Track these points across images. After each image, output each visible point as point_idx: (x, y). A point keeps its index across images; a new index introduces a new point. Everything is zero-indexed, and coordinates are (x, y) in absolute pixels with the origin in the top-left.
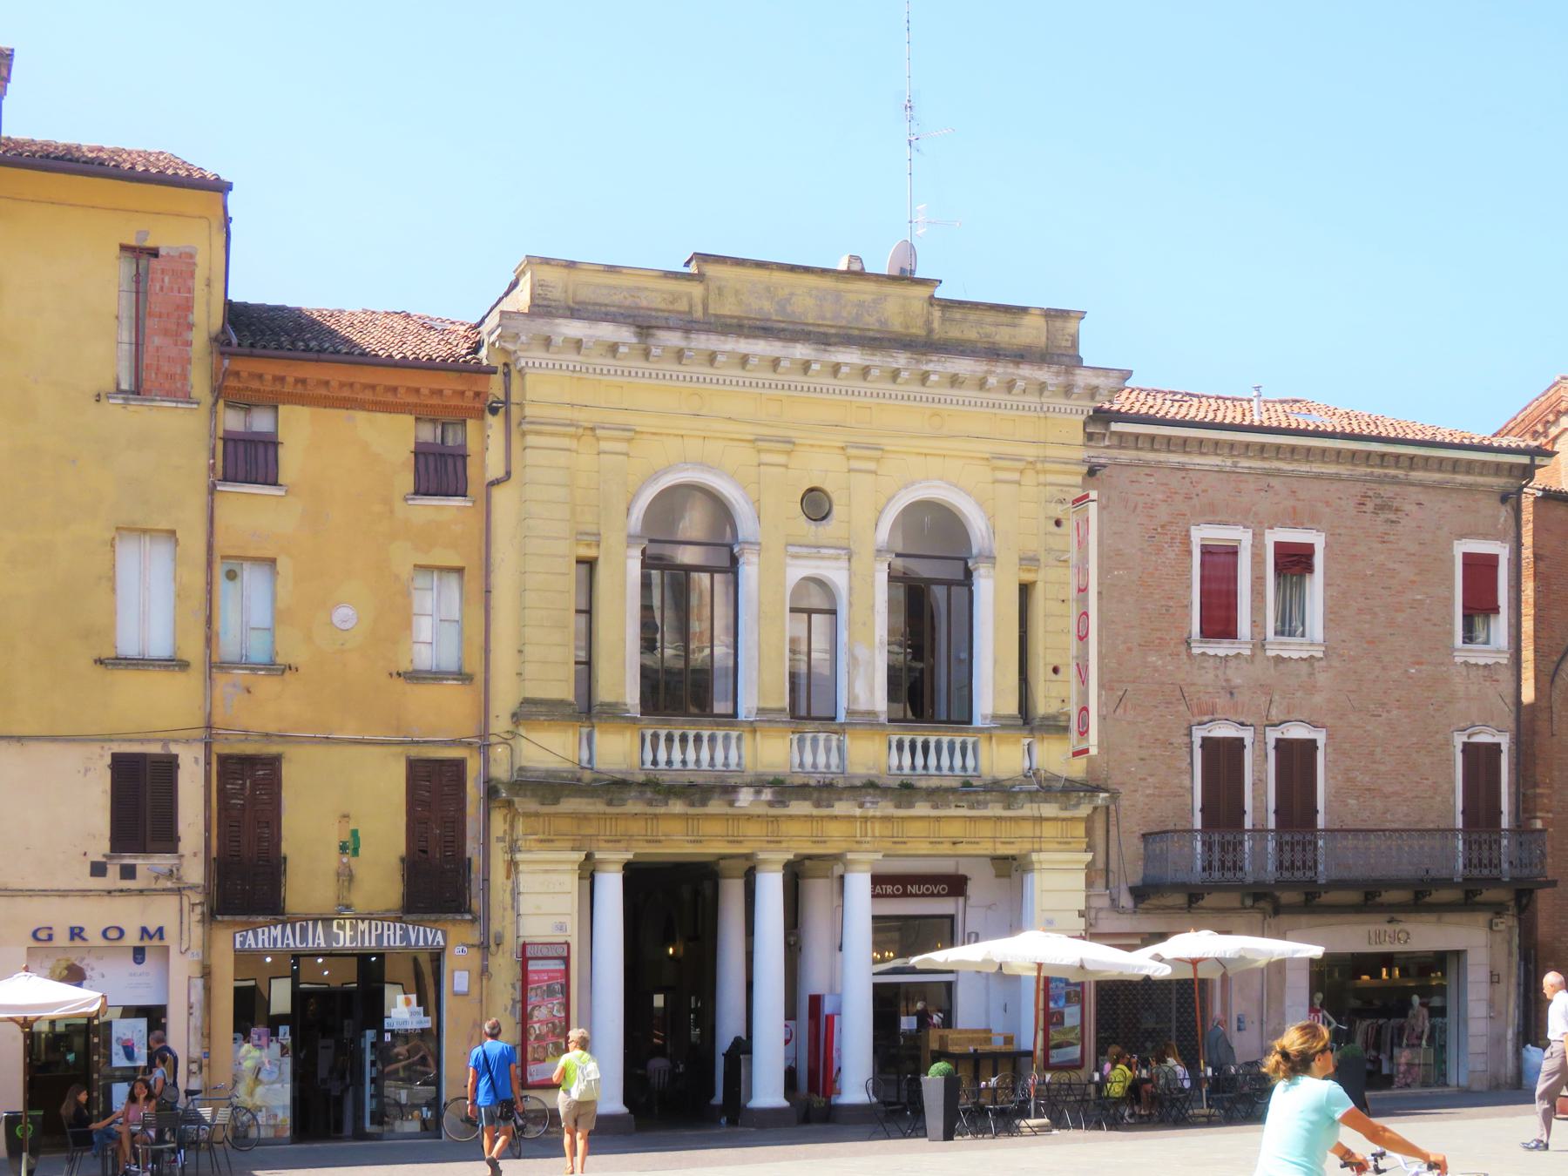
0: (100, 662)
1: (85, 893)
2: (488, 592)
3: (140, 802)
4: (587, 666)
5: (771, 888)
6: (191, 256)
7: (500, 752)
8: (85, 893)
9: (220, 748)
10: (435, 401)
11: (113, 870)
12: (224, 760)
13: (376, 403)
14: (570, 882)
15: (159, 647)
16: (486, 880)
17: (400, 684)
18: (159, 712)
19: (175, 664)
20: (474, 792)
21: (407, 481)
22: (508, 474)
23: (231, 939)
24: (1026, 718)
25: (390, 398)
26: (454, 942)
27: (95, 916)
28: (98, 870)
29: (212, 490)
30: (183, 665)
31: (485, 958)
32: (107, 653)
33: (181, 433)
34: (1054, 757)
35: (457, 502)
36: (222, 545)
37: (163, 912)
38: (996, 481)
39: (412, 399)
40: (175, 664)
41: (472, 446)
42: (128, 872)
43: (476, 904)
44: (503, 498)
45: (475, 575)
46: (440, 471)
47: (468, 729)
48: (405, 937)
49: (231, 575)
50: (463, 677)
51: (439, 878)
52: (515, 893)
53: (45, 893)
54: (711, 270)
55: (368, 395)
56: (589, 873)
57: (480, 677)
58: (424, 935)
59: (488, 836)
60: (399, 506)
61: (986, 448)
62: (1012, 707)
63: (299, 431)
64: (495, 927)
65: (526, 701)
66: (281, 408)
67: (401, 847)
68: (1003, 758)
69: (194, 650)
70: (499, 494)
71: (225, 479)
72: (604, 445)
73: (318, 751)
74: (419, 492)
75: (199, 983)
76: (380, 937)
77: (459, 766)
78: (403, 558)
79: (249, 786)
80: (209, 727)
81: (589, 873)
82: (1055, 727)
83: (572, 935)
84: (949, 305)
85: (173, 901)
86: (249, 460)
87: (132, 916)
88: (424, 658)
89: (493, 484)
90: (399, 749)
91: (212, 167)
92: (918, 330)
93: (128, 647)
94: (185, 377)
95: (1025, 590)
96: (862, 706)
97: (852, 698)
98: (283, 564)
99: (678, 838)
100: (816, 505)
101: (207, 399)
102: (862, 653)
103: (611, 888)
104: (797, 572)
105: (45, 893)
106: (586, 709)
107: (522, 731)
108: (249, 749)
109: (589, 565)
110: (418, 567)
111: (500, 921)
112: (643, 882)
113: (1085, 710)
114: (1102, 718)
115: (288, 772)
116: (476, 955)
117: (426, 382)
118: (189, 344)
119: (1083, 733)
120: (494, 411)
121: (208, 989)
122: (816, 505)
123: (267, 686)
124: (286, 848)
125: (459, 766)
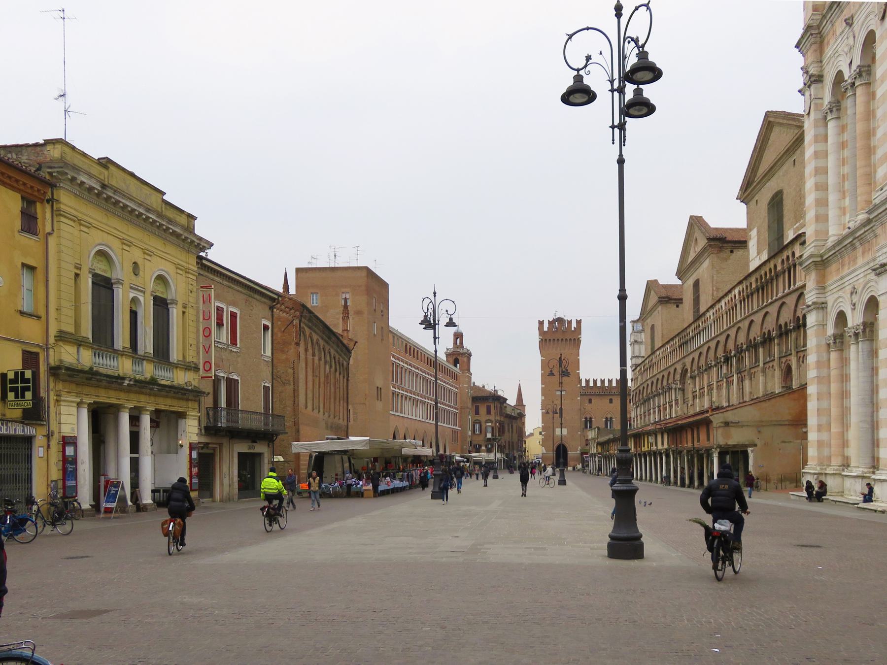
2: (47, 281)
7: (51, 352)
13: (10, 185)
16: (48, 407)
17: (18, 315)
20: (43, 369)
21: (18, 224)
22: (53, 230)
25: (15, 185)
26: (38, 434)
31: (49, 441)
39: (22, 187)
41: (39, 215)
44: (52, 241)
48: (23, 431)
54: (112, 168)
55: (7, 181)
58: (29, 431)
64: (51, 429)
65: (61, 331)
76: (15, 430)
89: (50, 234)
111: (53, 427)
116: (45, 439)
120: (48, 201)
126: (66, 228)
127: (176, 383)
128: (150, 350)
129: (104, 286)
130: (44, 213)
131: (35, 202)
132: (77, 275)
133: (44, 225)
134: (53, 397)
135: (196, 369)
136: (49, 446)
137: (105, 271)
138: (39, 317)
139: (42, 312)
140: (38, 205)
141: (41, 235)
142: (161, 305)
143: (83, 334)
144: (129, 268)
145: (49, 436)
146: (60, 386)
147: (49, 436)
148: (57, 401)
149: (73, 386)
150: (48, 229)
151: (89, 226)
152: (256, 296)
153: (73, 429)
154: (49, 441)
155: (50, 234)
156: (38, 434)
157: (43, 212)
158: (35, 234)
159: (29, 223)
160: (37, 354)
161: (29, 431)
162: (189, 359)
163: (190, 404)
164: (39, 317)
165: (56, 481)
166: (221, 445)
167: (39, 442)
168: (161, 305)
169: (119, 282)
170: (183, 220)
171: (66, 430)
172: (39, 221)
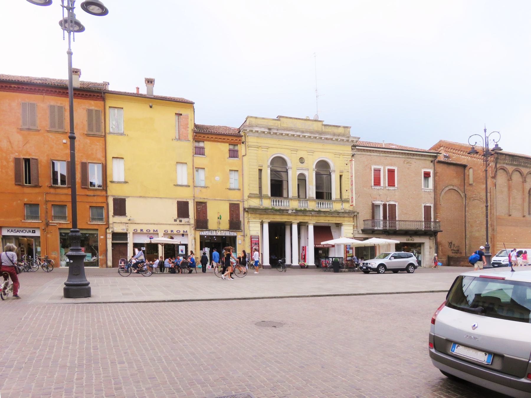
1: (173, 224)
3: (182, 209)
4: (260, 188)
5: (295, 228)
7: (246, 203)
8: (173, 224)
9: (197, 200)
10: (232, 141)
11: (178, 221)
12: (197, 202)
14: (259, 225)
15: (185, 183)
17: (228, 190)
18: (185, 195)
19: (188, 186)
20: (241, 210)
21: (228, 155)
23: (199, 233)
24: (341, 200)
27: (175, 229)
28: (175, 220)
30: (189, 186)
32: (175, 184)
33: (188, 146)
34: (347, 207)
36: (195, 166)
37: (187, 228)
40: (188, 186)
41: (239, 150)
42: (181, 221)
43: (242, 228)
46: (233, 154)
49: (197, 171)
50: (239, 190)
51: (235, 224)
52: (249, 227)
53: (166, 224)
56: (262, 224)
57: (242, 189)
59: (244, 217)
62: (339, 197)
63: (208, 146)
64: (246, 233)
67: (229, 219)
68: (337, 207)
69: (191, 184)
70: (244, 158)
75: (194, 240)
77: (238, 205)
78: (227, 169)
79: (202, 206)
81: (262, 224)
82: (347, 201)
83: (259, 234)
84: (325, 125)
85: (189, 226)
86: (199, 151)
87: (182, 229)
88: (232, 186)
91: (190, 99)
92: (320, 130)
93: (180, 183)
95: (341, 176)
96: (311, 196)
97: (309, 195)
99: (278, 219)
100: (302, 160)
102: (311, 187)
103: (266, 227)
104: (299, 172)
105: (166, 224)
106: (260, 196)
108: (201, 201)
109: (260, 170)
110: (230, 170)
112: (272, 226)
113: (352, 198)
114: (356, 199)
115: (208, 205)
116: (242, 237)
117: (230, 138)
119: (352, 202)
120: (243, 143)
121: (195, 241)
122: (302, 160)
123: (204, 190)
124: (208, 218)
125: (238, 205)
127: (332, 210)
134: (246, 221)
146: (250, 215)
148: (249, 222)
149: (258, 215)
151: (268, 148)
152: (414, 157)
156: (239, 236)
157: (241, 148)
158: (237, 157)
159: (233, 154)
161: (233, 234)
163: (346, 219)
164: (239, 190)
170: (341, 130)
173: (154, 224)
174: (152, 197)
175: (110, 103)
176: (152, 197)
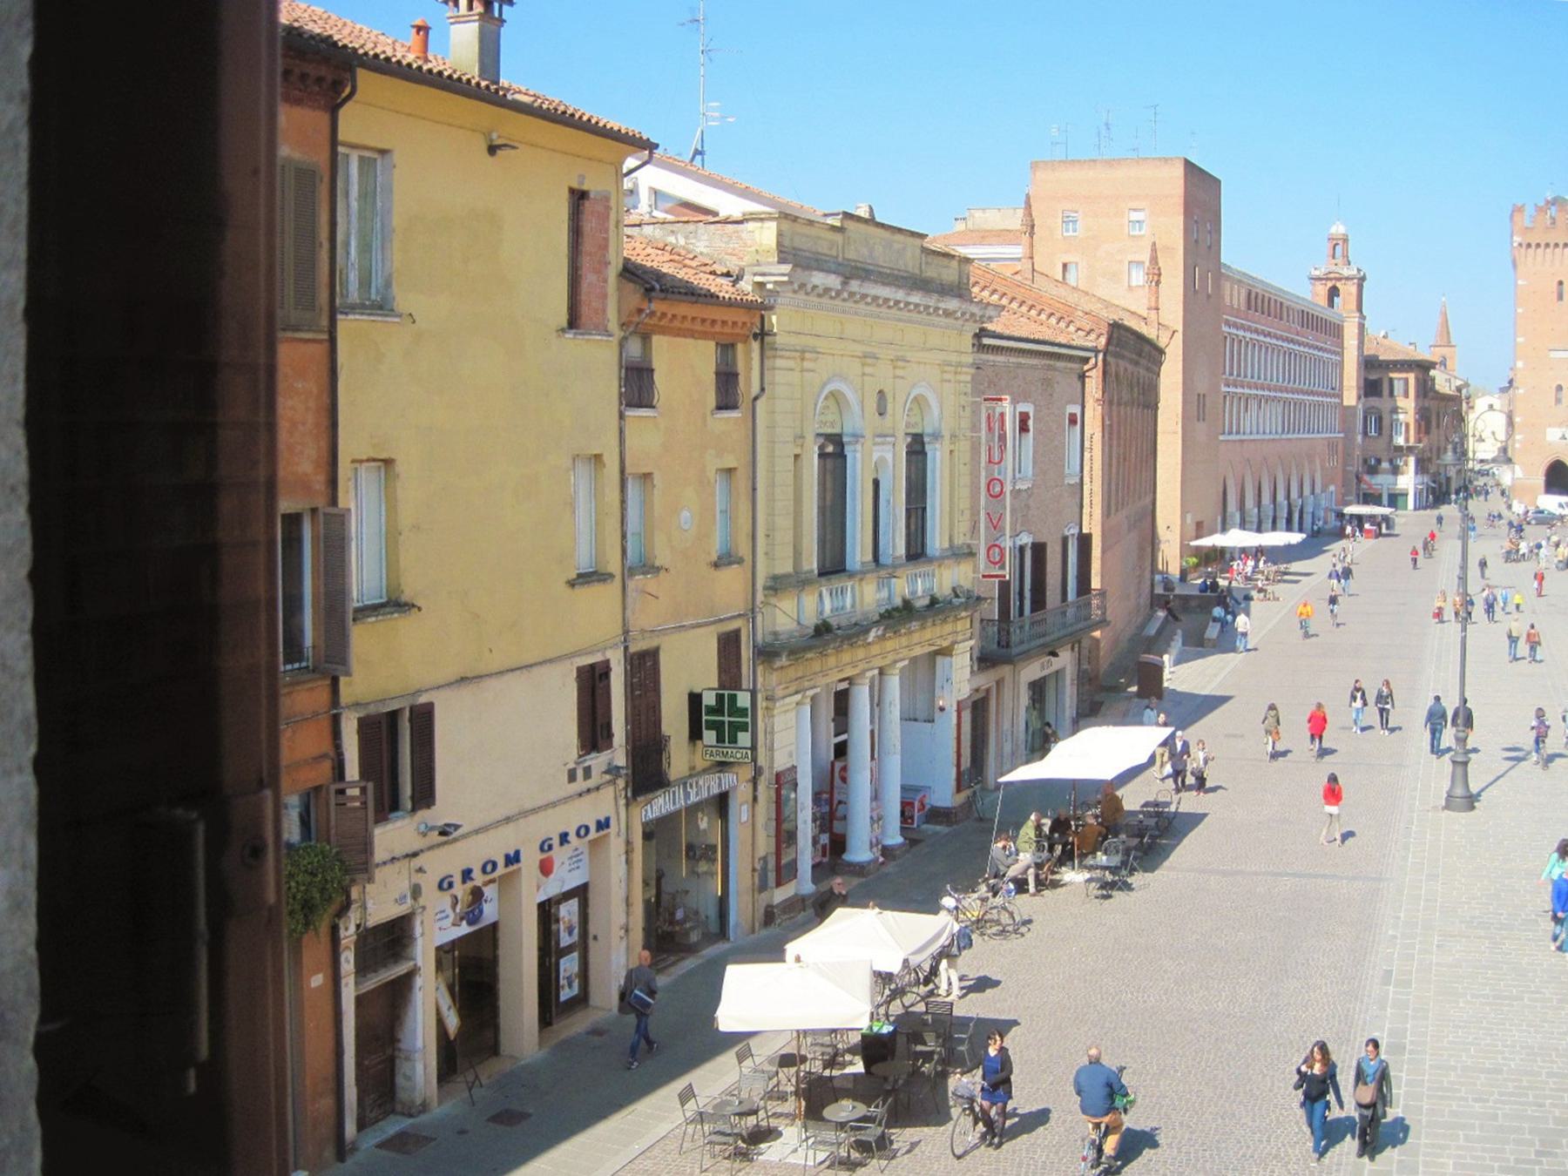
0: (572, 584)
2: (754, 489)
6: (607, 199)
7: (759, 618)
9: (632, 649)
11: (580, 773)
20: (746, 653)
21: (711, 399)
22: (763, 389)
28: (572, 777)
29: (621, 416)
30: (611, 576)
35: (734, 414)
38: (943, 381)
41: (741, 367)
45: (741, 477)
47: (740, 606)
57: (748, 559)
60: (709, 417)
61: (942, 356)
65: (775, 578)
66: (656, 339)
69: (614, 566)
71: (630, 405)
72: (807, 364)
73: (676, 637)
74: (719, 408)
80: (626, 632)
85: (611, 789)
87: (588, 812)
89: (756, 399)
90: (712, 628)
94: (604, 311)
98: (657, 479)
101: (618, 333)
107: (773, 600)
116: (750, 786)
118: (605, 281)
120: (755, 336)
126: (784, 374)
128: (901, 550)
129: (834, 453)
130: (749, 360)
131: (733, 345)
132: (797, 457)
133: (748, 379)
135: (971, 554)
136: (755, 799)
137: (832, 425)
138: (740, 561)
139: (744, 550)
140: (740, 347)
141: (745, 403)
142: (917, 450)
143: (806, 567)
144: (872, 403)
145: (754, 782)
147: (754, 782)
150: (755, 389)
153: (791, 755)
154: (755, 789)
155: (756, 399)
160: (737, 633)
162: (959, 540)
164: (740, 561)
165: (764, 859)
166: (999, 683)
167: (742, 793)
168: (917, 450)
169: (857, 437)
171: (781, 763)
172: (741, 379)
173: (508, 820)
174: (501, 673)
175: (354, 123)
176: (501, 673)
